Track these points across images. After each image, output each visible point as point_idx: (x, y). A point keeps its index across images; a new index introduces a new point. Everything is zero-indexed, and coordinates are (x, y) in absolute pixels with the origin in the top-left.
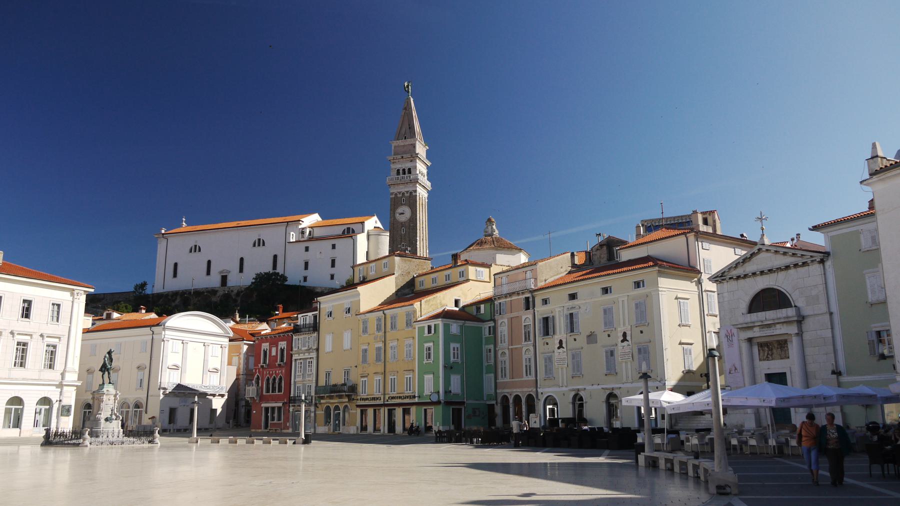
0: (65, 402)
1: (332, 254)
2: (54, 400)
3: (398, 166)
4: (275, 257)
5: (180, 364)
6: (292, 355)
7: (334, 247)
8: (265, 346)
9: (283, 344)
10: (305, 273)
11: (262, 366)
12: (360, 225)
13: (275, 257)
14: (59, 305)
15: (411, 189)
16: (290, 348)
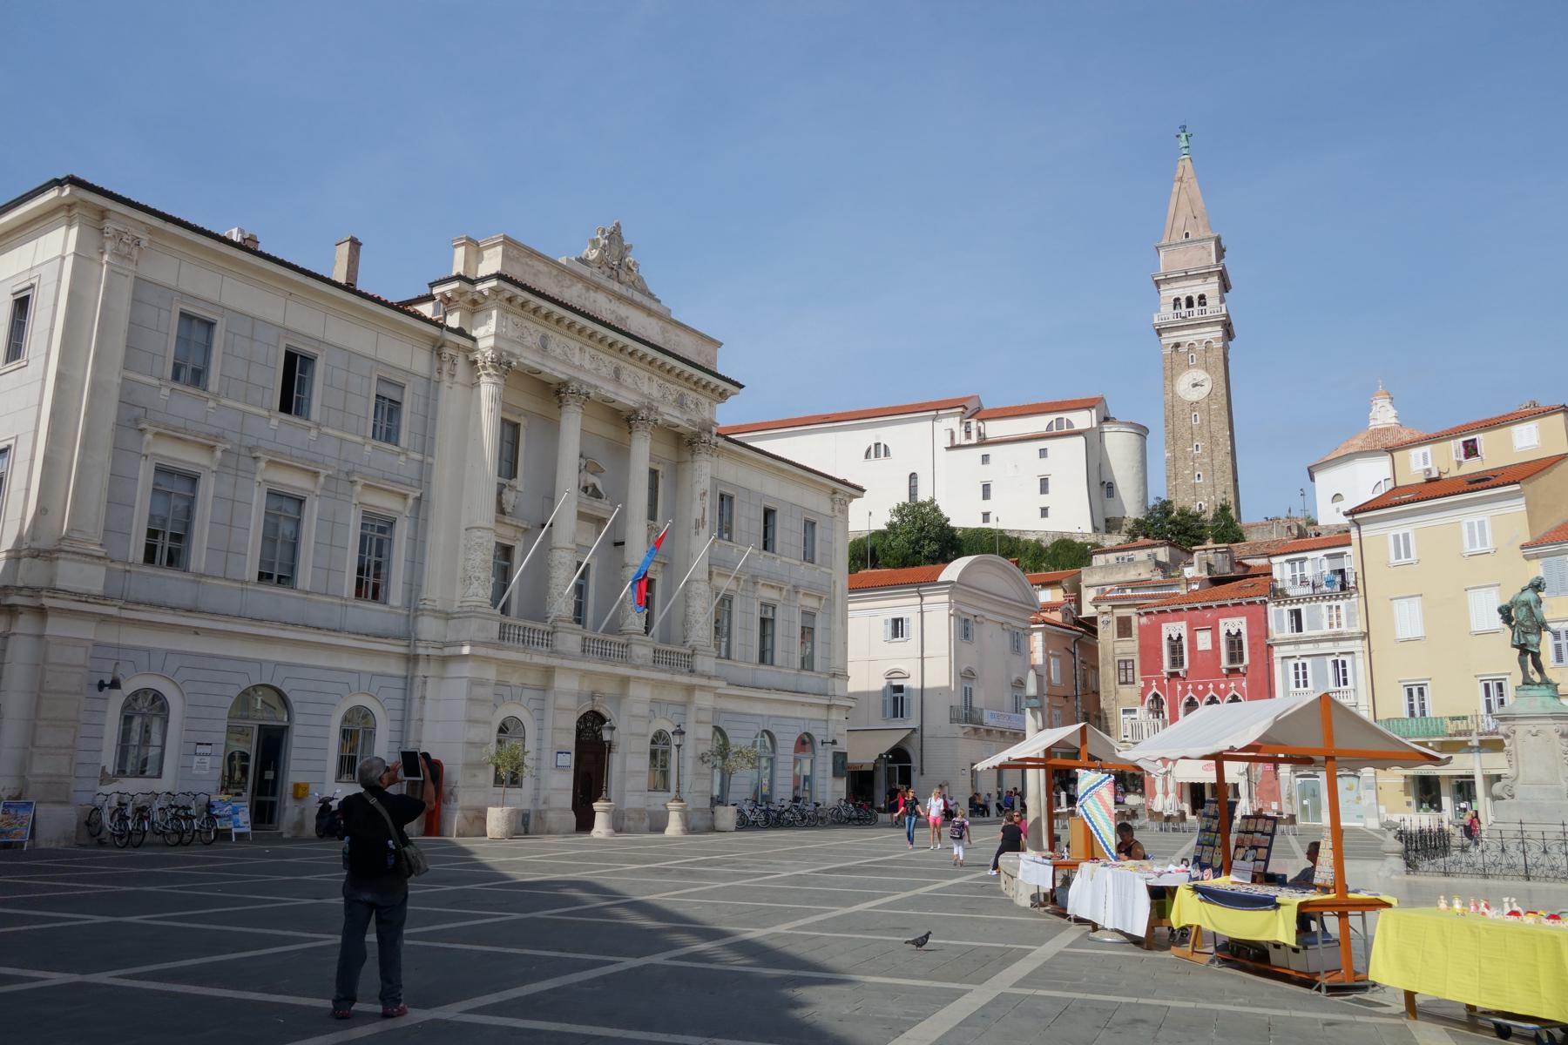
0: (840, 747)
1: (1043, 467)
2: (818, 739)
3: (1176, 293)
4: (913, 476)
5: (976, 670)
6: (1270, 646)
7: (1043, 453)
8: (1174, 628)
9: (1236, 624)
10: (986, 506)
11: (1174, 675)
12: (1085, 413)
13: (913, 476)
14: (813, 524)
15: (1208, 337)
16: (1260, 627)
